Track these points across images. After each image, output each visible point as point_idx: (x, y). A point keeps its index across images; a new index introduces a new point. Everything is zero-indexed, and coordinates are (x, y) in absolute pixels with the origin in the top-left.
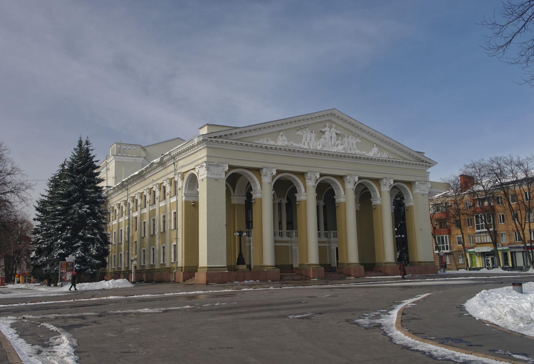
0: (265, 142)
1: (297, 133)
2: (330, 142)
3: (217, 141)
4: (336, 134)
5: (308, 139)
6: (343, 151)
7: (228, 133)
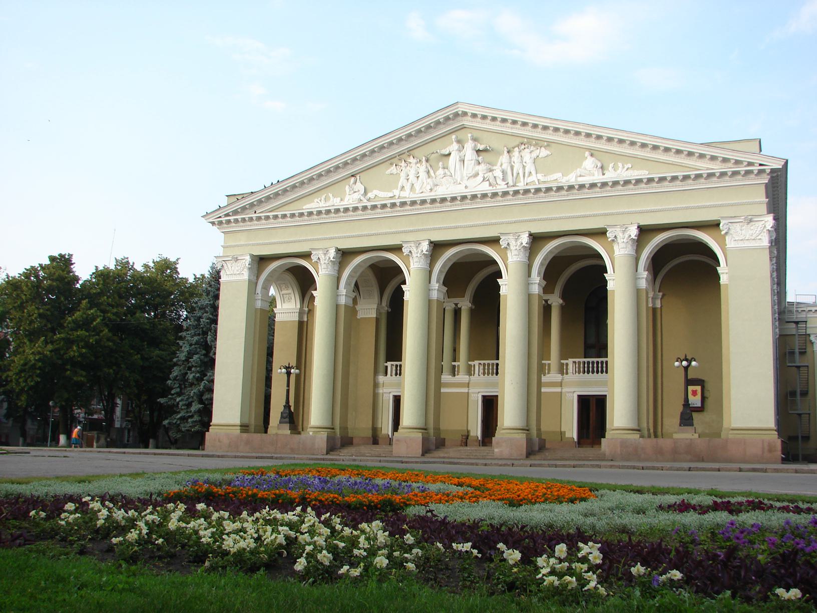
0: (322, 204)
1: (388, 172)
2: (462, 174)
3: (229, 222)
4: (478, 151)
5: (412, 177)
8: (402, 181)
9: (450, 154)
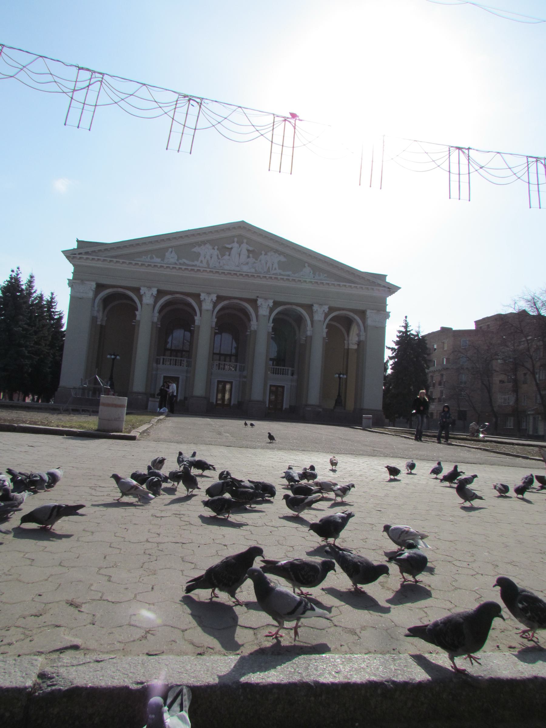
1: (194, 250)
4: (248, 250)
6: (253, 270)
7: (93, 249)
8: (201, 258)
9: (232, 248)
